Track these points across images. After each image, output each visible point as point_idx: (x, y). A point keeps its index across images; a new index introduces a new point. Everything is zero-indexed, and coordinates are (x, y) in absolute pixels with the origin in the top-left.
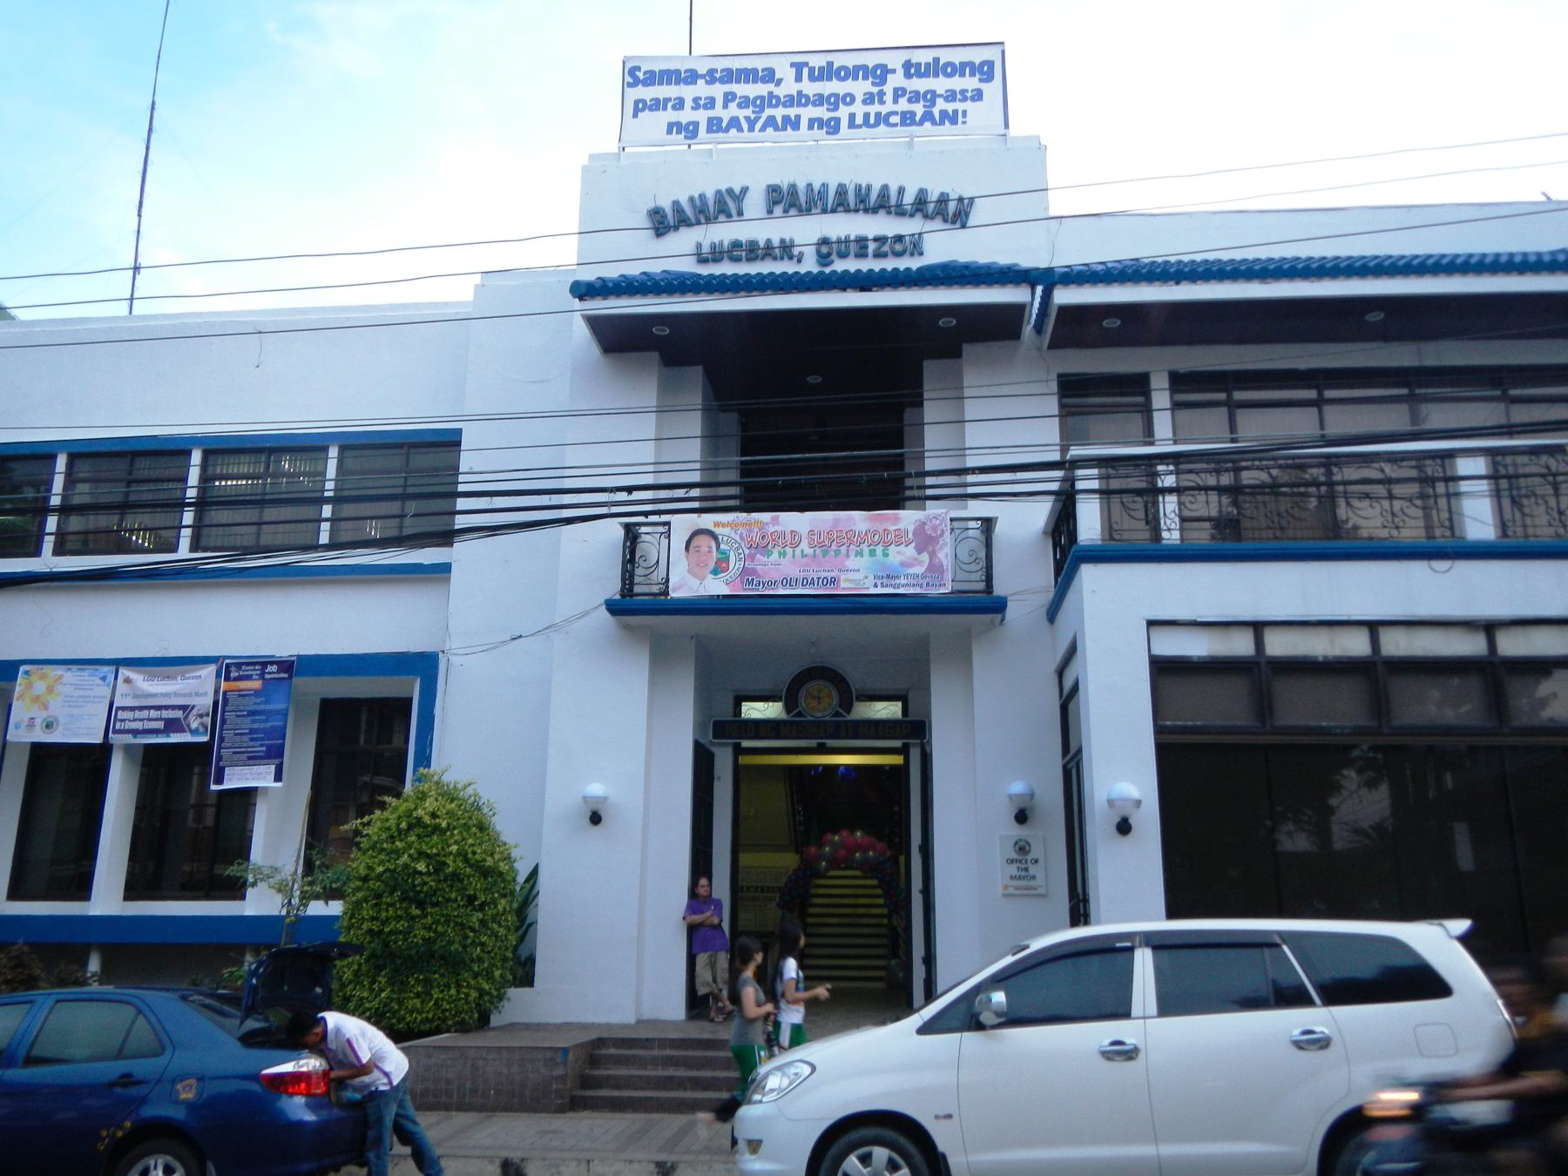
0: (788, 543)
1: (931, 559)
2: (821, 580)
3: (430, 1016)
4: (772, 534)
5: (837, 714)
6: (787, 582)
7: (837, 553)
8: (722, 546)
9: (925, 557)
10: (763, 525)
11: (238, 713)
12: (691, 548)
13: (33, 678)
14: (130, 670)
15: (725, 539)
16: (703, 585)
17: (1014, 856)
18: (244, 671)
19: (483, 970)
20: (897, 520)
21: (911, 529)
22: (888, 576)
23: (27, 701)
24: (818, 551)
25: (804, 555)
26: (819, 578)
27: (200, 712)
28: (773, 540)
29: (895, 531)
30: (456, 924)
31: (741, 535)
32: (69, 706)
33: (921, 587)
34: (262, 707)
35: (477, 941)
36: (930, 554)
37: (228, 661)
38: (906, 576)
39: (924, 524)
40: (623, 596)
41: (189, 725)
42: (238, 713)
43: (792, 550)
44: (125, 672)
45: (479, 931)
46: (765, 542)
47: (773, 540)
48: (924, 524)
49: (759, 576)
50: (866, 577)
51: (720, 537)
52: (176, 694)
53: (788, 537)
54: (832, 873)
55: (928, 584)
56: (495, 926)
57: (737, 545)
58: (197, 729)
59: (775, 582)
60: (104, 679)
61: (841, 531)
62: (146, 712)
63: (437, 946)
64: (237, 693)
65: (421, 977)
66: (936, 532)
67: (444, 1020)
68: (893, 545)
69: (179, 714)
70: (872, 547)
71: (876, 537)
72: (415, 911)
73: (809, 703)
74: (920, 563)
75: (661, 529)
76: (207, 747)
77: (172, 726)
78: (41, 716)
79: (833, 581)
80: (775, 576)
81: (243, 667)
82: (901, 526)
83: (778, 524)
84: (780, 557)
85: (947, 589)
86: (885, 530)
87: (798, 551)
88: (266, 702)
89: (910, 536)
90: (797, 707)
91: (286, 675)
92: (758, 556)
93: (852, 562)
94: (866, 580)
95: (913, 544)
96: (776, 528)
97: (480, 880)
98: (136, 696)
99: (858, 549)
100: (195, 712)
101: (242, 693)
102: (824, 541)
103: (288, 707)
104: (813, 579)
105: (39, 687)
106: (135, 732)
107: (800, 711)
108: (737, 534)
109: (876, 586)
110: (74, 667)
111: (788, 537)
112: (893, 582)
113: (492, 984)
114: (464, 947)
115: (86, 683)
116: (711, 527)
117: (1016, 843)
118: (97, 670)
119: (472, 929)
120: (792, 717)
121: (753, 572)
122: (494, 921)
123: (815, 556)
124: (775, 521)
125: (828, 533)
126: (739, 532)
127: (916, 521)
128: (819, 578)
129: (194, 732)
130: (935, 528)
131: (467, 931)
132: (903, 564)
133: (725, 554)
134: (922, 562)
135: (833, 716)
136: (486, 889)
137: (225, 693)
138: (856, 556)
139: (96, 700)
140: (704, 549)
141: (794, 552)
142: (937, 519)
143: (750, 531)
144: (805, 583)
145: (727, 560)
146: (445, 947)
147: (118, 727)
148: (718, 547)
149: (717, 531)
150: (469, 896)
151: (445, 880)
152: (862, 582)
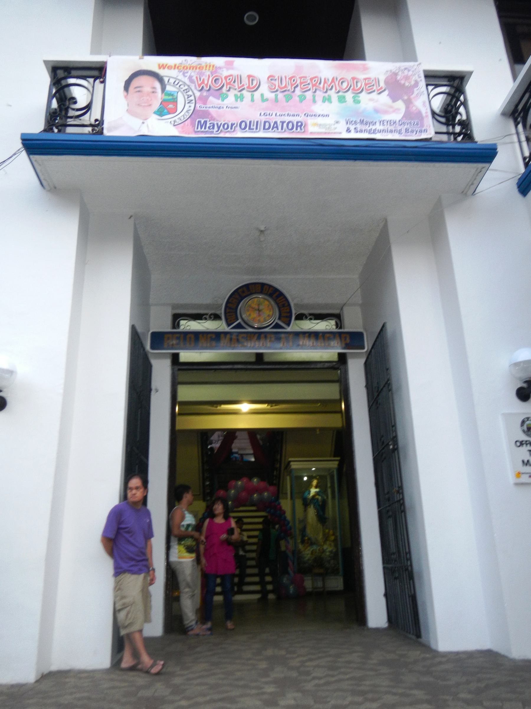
0: (245, 87)
1: (407, 108)
2: (285, 125)
4: (226, 78)
5: (277, 326)
6: (245, 125)
7: (302, 99)
8: (169, 88)
9: (400, 105)
10: (215, 69)
12: (131, 88)
15: (172, 81)
16: (145, 125)
17: (524, 437)
20: (365, 69)
21: (382, 78)
22: (362, 122)
24: (280, 96)
25: (263, 99)
26: (283, 123)
28: (227, 84)
29: (365, 79)
31: (190, 78)
33: (400, 132)
36: (405, 101)
38: (382, 122)
39: (396, 74)
40: (48, 129)
43: (250, 94)
46: (218, 86)
47: (227, 84)
48: (396, 74)
49: (213, 118)
50: (337, 122)
51: (166, 79)
53: (245, 81)
54: (235, 509)
55: (407, 130)
57: (186, 87)
59: (232, 125)
61: (306, 77)
66: (410, 83)
68: (364, 93)
70: (340, 94)
71: (345, 85)
73: (250, 315)
74: (396, 110)
75: (96, 73)
79: (300, 125)
80: (230, 118)
82: (372, 75)
83: (232, 69)
84: (236, 100)
85: (430, 134)
86: (353, 79)
87: (257, 94)
89: (382, 84)
90: (238, 320)
92: (211, 98)
93: (319, 108)
94: (336, 125)
95: (386, 92)
96: (230, 72)
99: (326, 95)
102: (286, 86)
104: (276, 123)
107: (239, 323)
108: (185, 76)
109: (348, 130)
111: (245, 81)
112: (367, 127)
116: (156, 69)
117: (523, 422)
120: (233, 328)
121: (206, 114)
123: (276, 100)
124: (229, 66)
125: (290, 79)
126: (188, 75)
127: (387, 71)
128: (283, 123)
130: (407, 78)
132: (376, 111)
133: (172, 95)
134: (398, 109)
135: (273, 328)
138: (324, 101)
140: (147, 89)
141: (253, 96)
142: (409, 71)
143: (201, 74)
144: (267, 127)
145: (175, 102)
148: (163, 89)
149: (162, 72)
152: (333, 127)
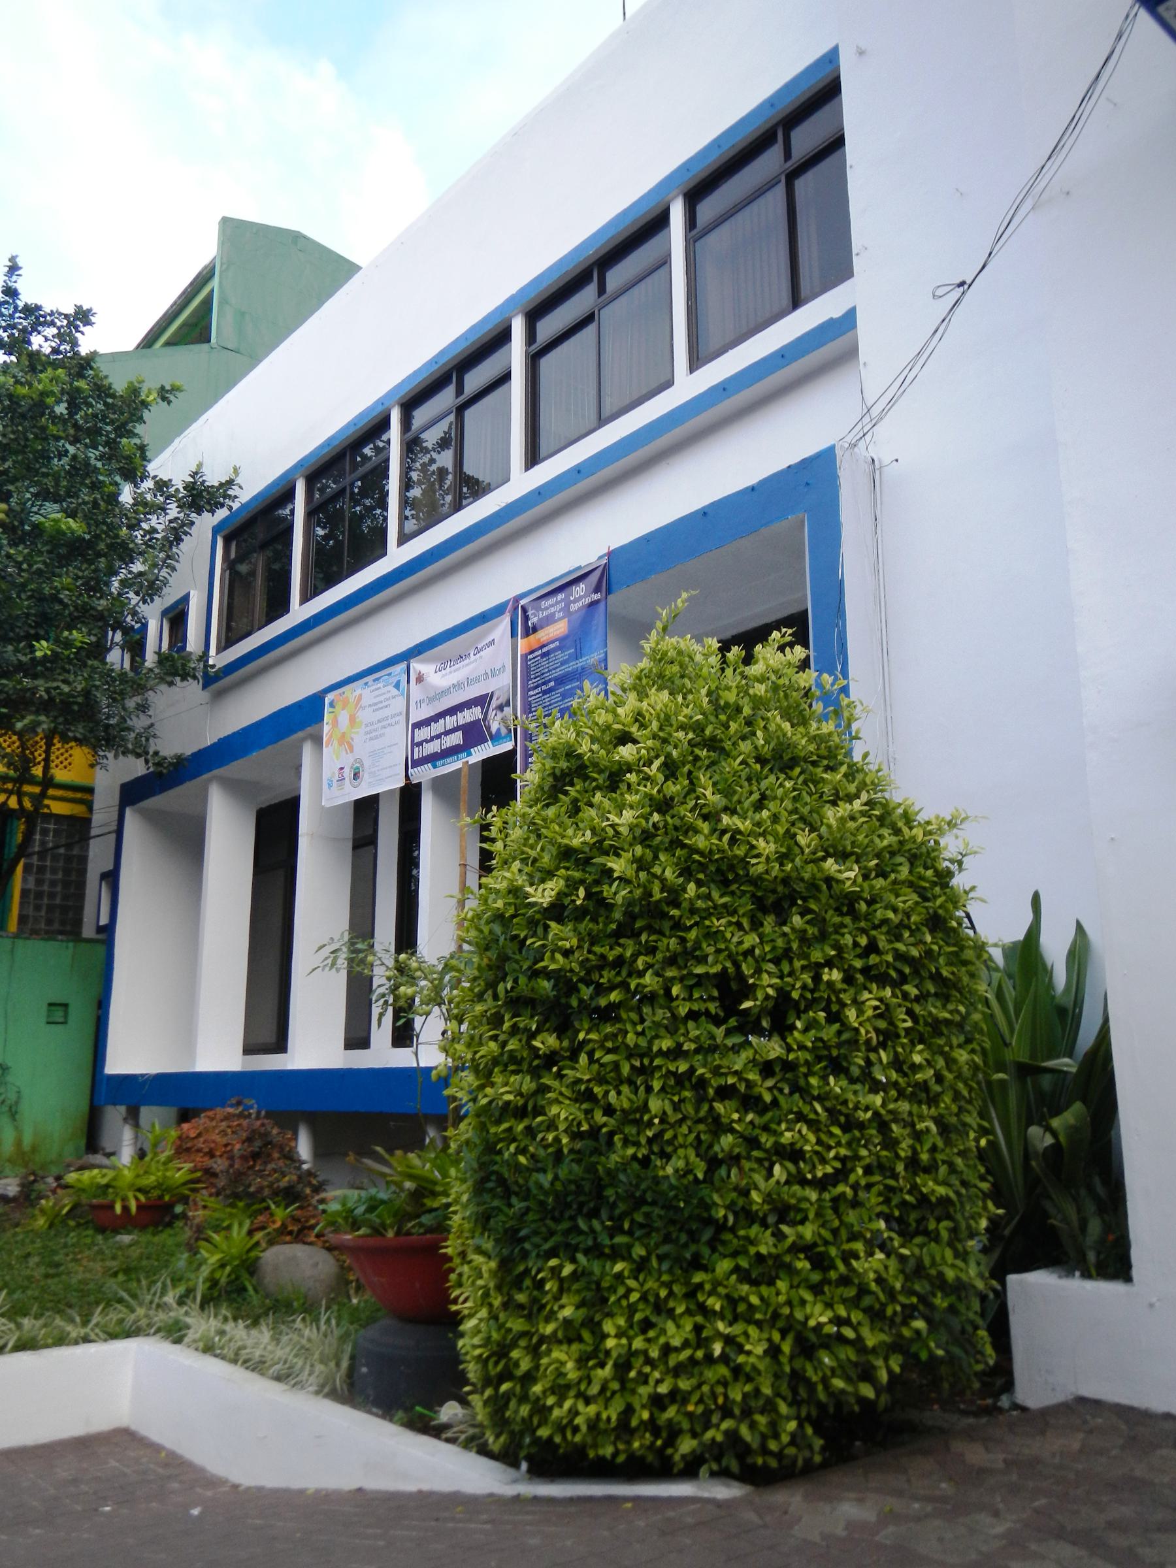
3: (613, 1413)
11: (544, 688)
13: (338, 707)
14: (423, 661)
18: (547, 608)
19: (795, 1249)
23: (336, 743)
27: (499, 702)
30: (681, 1080)
32: (371, 739)
34: (573, 666)
35: (767, 1140)
37: (522, 602)
41: (488, 728)
42: (544, 688)
44: (417, 666)
45: (775, 1103)
52: (470, 681)
56: (835, 1084)
58: (498, 730)
60: (397, 686)
62: (442, 721)
63: (615, 1158)
64: (539, 652)
65: (567, 1270)
67: (673, 1434)
69: (474, 714)
72: (547, 1042)
76: (513, 752)
77: (474, 734)
78: (348, 761)
81: (543, 604)
88: (577, 656)
91: (598, 596)
97: (756, 925)
98: (430, 700)
100: (494, 704)
101: (545, 650)
103: (606, 653)
105: (343, 717)
106: (433, 759)
110: (370, 679)
113: (853, 1303)
114: (714, 1163)
115: (382, 698)
118: (389, 675)
119: (749, 1102)
122: (838, 1067)
129: (496, 738)
131: (719, 1107)
136: (787, 954)
137: (525, 657)
139: (394, 720)
146: (645, 1162)
147: (416, 757)
150: (721, 979)
151: (625, 930)
